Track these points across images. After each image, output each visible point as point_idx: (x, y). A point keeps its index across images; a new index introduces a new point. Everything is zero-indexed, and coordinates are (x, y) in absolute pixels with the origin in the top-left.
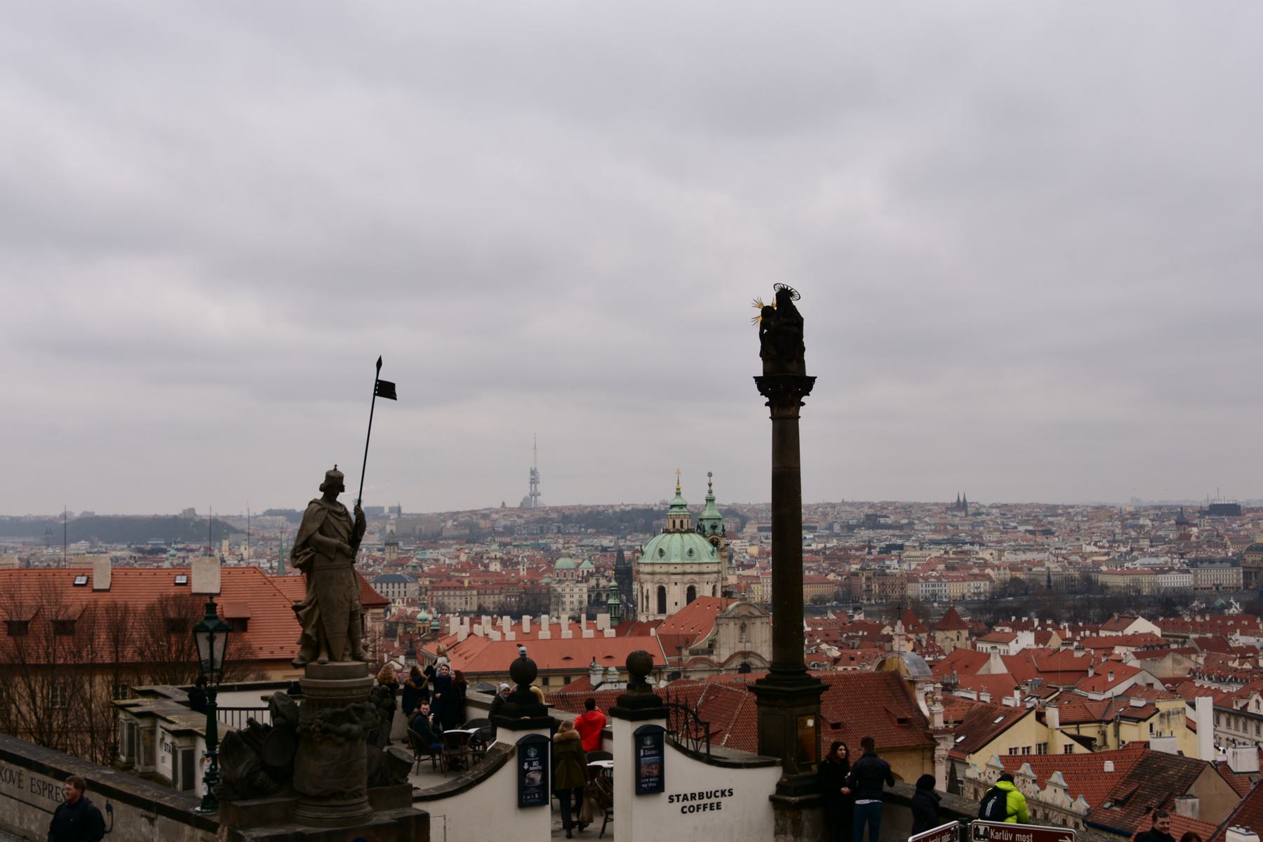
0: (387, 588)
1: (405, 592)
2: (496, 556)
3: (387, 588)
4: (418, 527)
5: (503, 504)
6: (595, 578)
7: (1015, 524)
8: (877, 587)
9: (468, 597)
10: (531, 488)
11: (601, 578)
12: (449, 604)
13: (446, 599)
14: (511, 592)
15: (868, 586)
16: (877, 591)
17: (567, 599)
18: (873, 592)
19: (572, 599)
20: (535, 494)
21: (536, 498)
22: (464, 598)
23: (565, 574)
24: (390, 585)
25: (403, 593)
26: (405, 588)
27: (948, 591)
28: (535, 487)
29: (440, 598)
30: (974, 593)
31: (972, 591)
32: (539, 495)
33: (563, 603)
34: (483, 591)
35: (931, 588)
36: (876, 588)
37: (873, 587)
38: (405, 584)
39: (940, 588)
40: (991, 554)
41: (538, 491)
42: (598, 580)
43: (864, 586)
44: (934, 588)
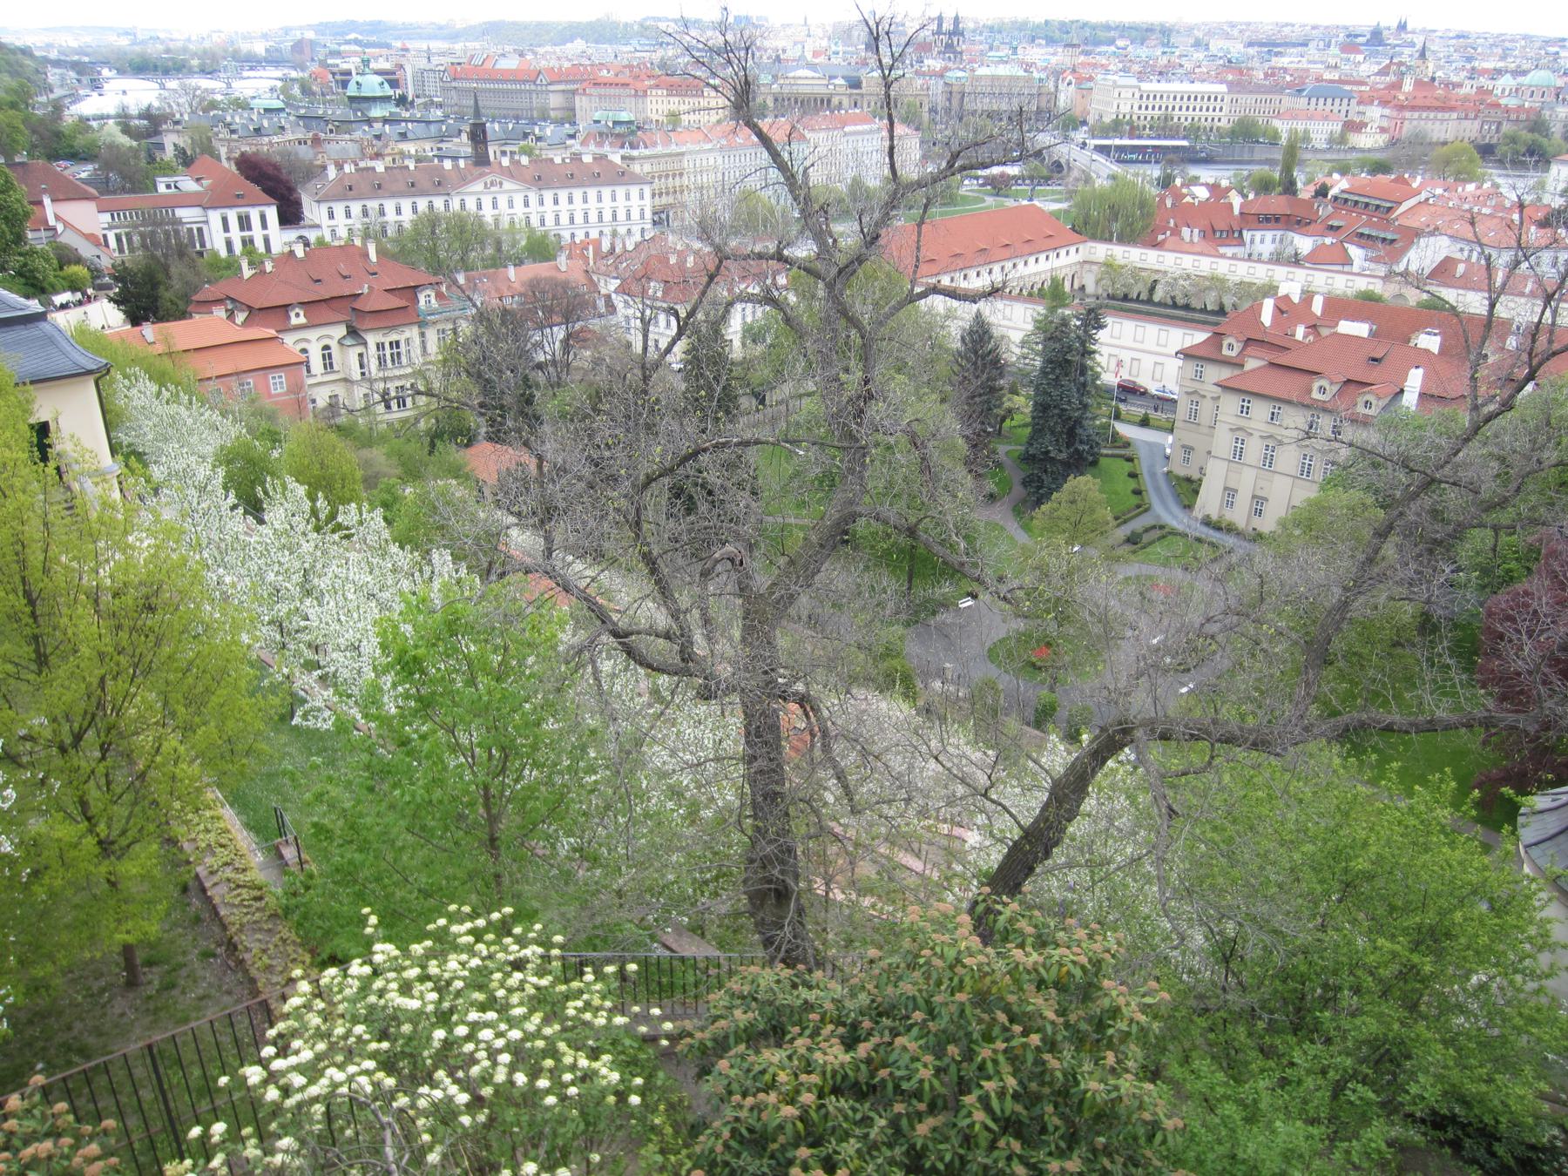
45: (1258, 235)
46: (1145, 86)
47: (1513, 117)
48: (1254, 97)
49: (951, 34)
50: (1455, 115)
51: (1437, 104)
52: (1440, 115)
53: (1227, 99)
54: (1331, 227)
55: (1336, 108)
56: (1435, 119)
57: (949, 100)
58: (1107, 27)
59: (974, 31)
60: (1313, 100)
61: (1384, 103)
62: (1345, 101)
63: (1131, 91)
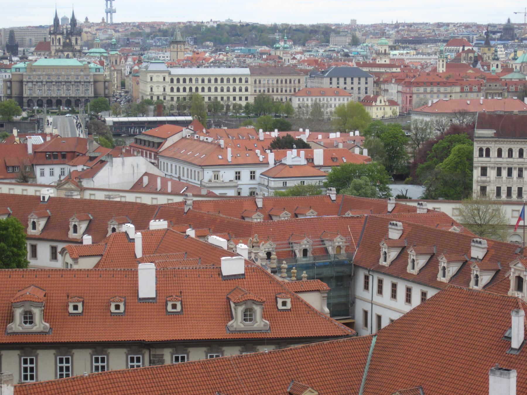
0: (345, 83)
1: (366, 89)
3: (345, 83)
4: (28, 38)
5: (87, 19)
10: (107, 6)
14: (494, 89)
20: (110, 11)
21: (111, 14)
24: (349, 80)
26: (366, 83)
28: (111, 4)
32: (115, 12)
34: (514, 87)
38: (366, 79)
41: (114, 8)
45: (47, 169)
46: (176, 71)
47: (512, 88)
48: (275, 78)
49: (70, 34)
50: (458, 89)
51: (438, 80)
52: (442, 89)
53: (251, 80)
54: (92, 159)
55: (349, 86)
56: (432, 92)
57: (10, 88)
58: (274, 29)
59: (148, 35)
60: (334, 80)
61: (399, 81)
62: (363, 80)
63: (161, 76)
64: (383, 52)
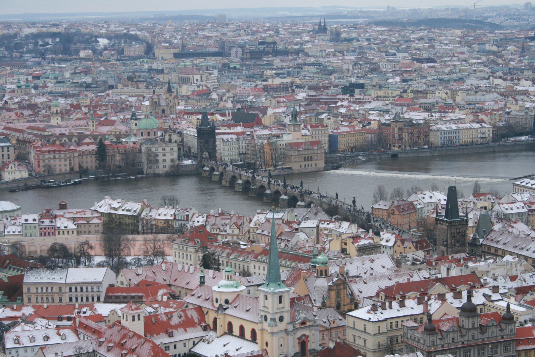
1: (8, 155)
2: (57, 111)
6: (168, 134)
7: (394, 51)
8: (407, 135)
9: (72, 159)
11: (173, 134)
12: (55, 166)
13: (52, 161)
15: (399, 135)
16: (407, 140)
17: (160, 158)
18: (404, 140)
19: (164, 158)
22: (68, 160)
23: (149, 133)
25: (7, 156)
26: (8, 151)
27: (461, 137)
29: (47, 161)
30: (481, 138)
31: (479, 136)
33: (157, 161)
35: (448, 135)
36: (405, 136)
37: (404, 136)
39: (455, 135)
40: (446, 93)
42: (170, 135)
43: (396, 135)
44: (450, 135)
64: (55, 112)
